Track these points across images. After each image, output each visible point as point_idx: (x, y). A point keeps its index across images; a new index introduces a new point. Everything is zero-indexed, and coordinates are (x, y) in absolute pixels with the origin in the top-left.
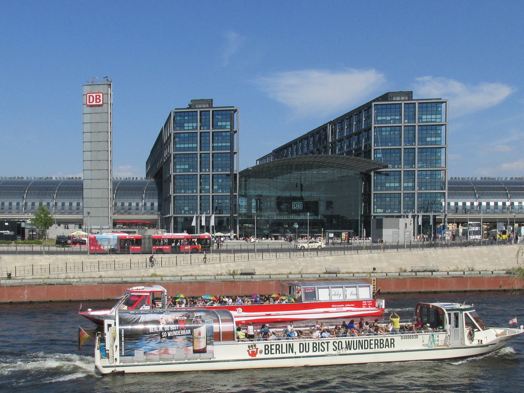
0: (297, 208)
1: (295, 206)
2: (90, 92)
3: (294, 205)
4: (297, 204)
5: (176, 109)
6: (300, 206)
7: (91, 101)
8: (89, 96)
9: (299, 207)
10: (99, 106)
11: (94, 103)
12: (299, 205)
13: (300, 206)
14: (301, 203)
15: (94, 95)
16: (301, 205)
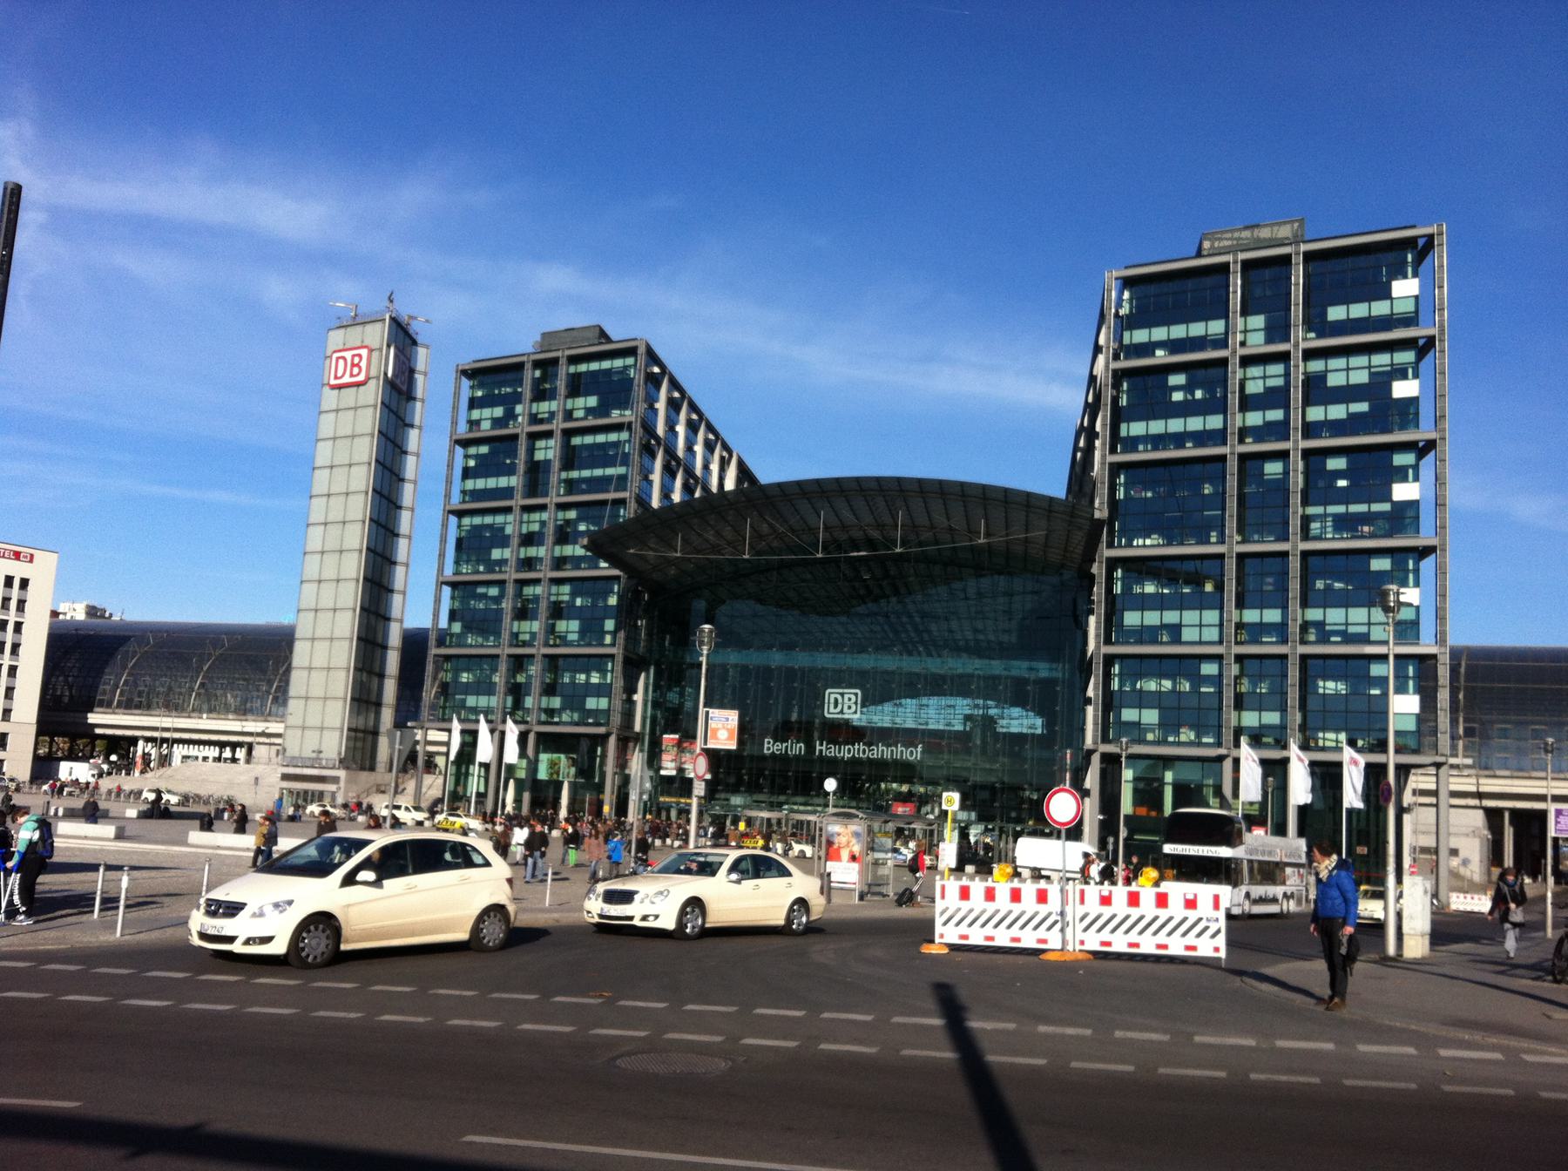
0: (842, 712)
1: (836, 706)
2: (341, 347)
3: (832, 700)
4: (842, 695)
5: (474, 362)
6: (854, 707)
7: (339, 375)
8: (338, 358)
9: (850, 707)
10: (358, 385)
11: (347, 379)
12: (850, 699)
13: (854, 707)
14: (856, 694)
15: (348, 355)
16: (856, 703)
